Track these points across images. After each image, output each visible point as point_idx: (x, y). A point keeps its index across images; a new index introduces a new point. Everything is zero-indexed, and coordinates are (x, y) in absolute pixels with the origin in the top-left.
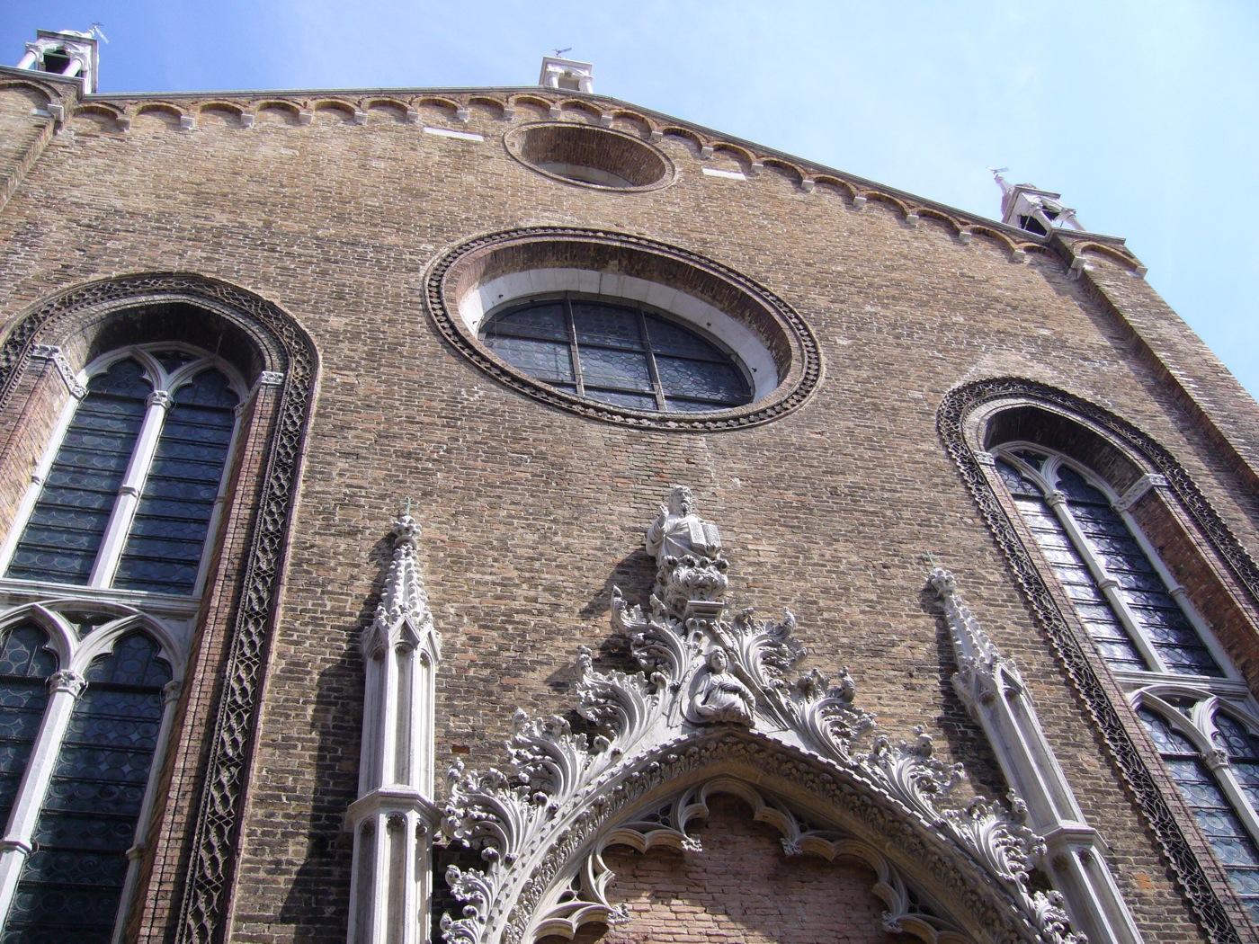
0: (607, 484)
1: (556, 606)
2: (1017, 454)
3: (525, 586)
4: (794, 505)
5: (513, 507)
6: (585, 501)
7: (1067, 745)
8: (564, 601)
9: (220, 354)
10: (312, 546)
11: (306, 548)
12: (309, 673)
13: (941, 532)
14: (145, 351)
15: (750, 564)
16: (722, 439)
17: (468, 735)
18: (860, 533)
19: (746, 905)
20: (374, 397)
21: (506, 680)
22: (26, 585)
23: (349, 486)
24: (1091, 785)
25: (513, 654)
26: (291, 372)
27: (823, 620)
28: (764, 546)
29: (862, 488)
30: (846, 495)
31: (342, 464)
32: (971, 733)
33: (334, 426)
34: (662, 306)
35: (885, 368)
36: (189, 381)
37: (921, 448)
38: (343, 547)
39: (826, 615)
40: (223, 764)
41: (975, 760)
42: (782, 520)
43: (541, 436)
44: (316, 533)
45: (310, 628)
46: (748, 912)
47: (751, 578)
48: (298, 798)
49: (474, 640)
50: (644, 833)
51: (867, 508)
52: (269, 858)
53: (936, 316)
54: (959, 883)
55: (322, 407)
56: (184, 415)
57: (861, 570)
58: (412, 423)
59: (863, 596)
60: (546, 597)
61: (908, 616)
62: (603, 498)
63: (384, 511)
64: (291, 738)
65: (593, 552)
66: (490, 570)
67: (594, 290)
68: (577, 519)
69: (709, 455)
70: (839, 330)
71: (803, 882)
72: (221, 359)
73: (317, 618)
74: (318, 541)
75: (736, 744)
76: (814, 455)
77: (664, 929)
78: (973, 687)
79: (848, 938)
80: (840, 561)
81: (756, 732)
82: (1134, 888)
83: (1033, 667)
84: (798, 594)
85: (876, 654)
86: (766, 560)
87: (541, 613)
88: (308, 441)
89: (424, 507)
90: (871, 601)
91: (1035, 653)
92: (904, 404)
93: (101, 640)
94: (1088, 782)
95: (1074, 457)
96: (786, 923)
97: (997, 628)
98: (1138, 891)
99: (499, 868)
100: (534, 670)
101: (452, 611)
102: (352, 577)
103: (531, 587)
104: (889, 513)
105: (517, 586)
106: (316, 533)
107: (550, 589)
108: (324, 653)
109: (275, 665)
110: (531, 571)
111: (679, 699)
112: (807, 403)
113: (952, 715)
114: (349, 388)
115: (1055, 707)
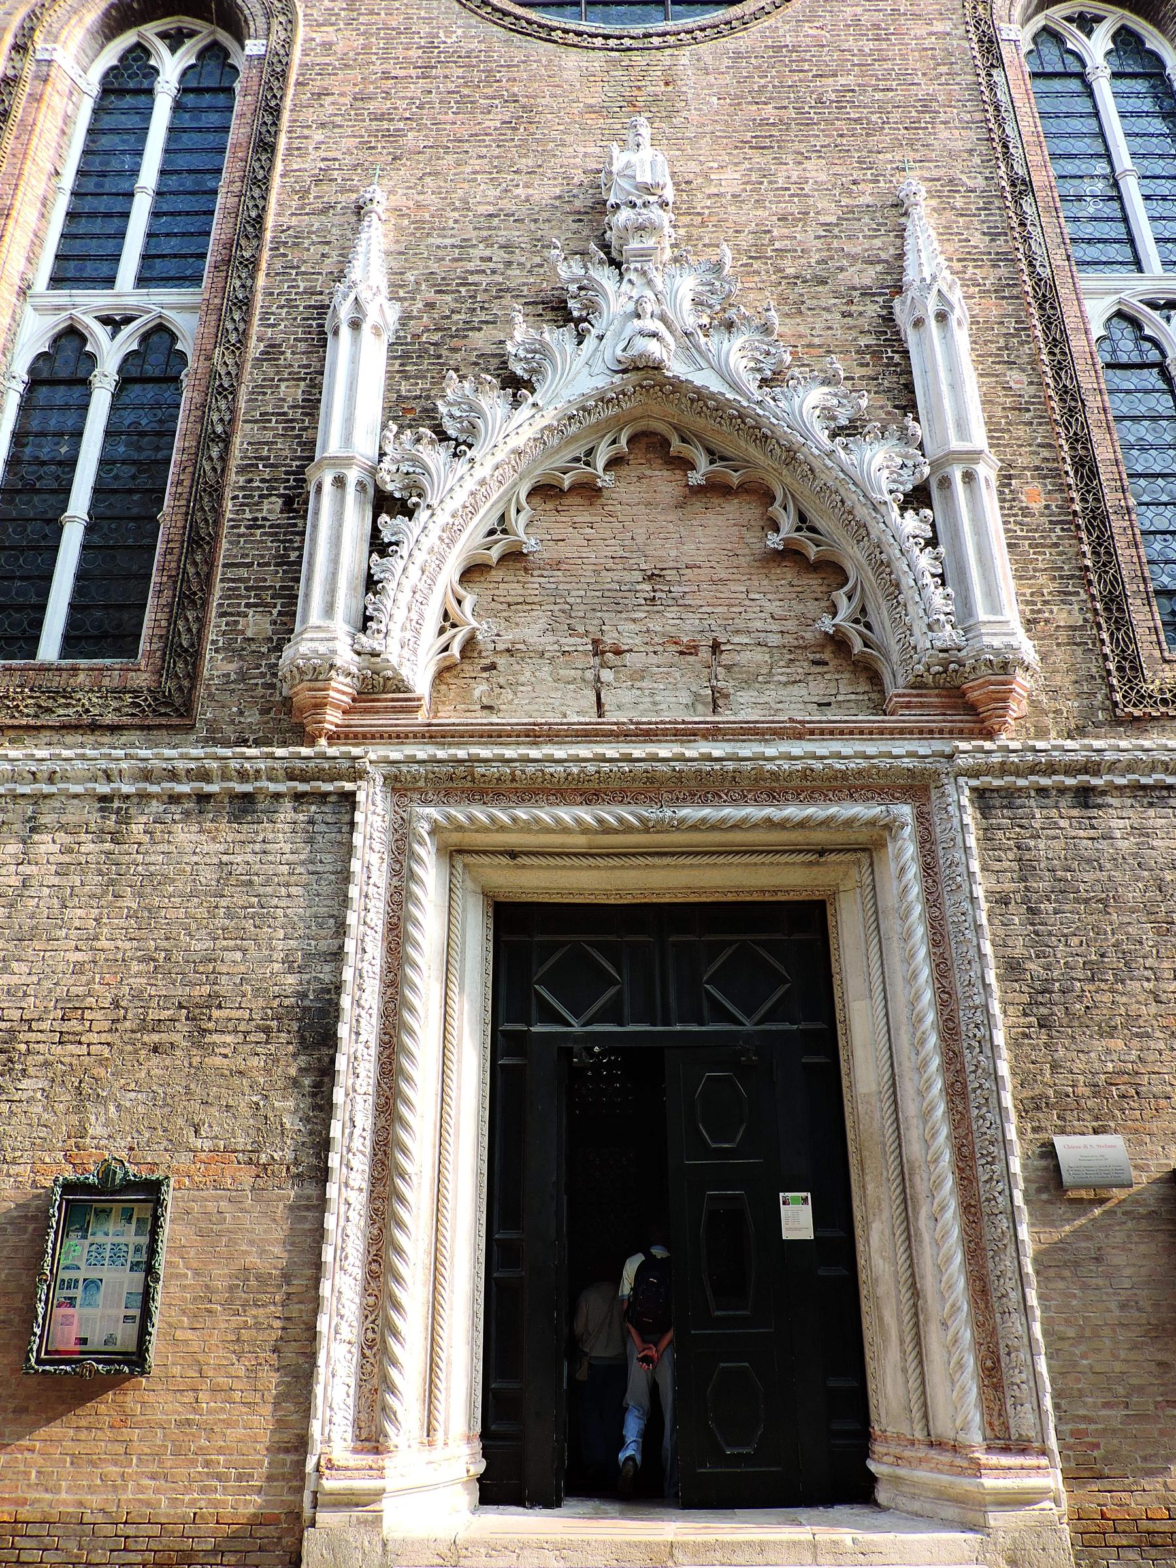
1: (509, 264)
2: (1069, 19)
3: (481, 246)
4: (771, 121)
5: (479, 161)
7: (999, 363)
8: (518, 257)
9: (218, 25)
10: (289, 228)
11: (283, 231)
12: (283, 353)
14: (149, 31)
15: (709, 196)
17: (416, 397)
20: (351, 54)
21: (455, 342)
22: (62, 296)
23: (323, 160)
25: (463, 316)
26: (273, 37)
27: (773, 250)
29: (853, 91)
31: (318, 136)
33: (313, 94)
36: (193, 61)
37: (934, 29)
38: (316, 225)
39: (777, 245)
40: (213, 440)
41: (895, 386)
43: (516, 75)
44: (293, 214)
45: (285, 310)
47: (707, 211)
48: (272, 465)
49: (430, 306)
50: (564, 473)
51: (852, 116)
52: (248, 516)
54: (839, 504)
55: (303, 75)
56: (190, 99)
57: (827, 189)
58: (387, 78)
60: (499, 255)
62: (569, 139)
63: (355, 182)
64: (266, 414)
66: (451, 232)
72: (219, 29)
73: (291, 300)
74: (294, 221)
75: (653, 386)
76: (808, 56)
77: (576, 555)
80: (807, 182)
81: (670, 374)
84: (753, 224)
85: (823, 282)
87: (494, 272)
88: (286, 116)
89: (392, 173)
91: (994, 266)
93: (128, 340)
95: (1138, 13)
98: (1024, 505)
99: (422, 515)
100: (480, 329)
101: (412, 279)
102: (323, 255)
103: (487, 246)
104: (874, 118)
105: (474, 246)
106: (293, 214)
107: (507, 247)
108: (296, 333)
109: (255, 348)
110: (489, 228)
111: (601, 347)
113: (885, 340)
114: (327, 46)
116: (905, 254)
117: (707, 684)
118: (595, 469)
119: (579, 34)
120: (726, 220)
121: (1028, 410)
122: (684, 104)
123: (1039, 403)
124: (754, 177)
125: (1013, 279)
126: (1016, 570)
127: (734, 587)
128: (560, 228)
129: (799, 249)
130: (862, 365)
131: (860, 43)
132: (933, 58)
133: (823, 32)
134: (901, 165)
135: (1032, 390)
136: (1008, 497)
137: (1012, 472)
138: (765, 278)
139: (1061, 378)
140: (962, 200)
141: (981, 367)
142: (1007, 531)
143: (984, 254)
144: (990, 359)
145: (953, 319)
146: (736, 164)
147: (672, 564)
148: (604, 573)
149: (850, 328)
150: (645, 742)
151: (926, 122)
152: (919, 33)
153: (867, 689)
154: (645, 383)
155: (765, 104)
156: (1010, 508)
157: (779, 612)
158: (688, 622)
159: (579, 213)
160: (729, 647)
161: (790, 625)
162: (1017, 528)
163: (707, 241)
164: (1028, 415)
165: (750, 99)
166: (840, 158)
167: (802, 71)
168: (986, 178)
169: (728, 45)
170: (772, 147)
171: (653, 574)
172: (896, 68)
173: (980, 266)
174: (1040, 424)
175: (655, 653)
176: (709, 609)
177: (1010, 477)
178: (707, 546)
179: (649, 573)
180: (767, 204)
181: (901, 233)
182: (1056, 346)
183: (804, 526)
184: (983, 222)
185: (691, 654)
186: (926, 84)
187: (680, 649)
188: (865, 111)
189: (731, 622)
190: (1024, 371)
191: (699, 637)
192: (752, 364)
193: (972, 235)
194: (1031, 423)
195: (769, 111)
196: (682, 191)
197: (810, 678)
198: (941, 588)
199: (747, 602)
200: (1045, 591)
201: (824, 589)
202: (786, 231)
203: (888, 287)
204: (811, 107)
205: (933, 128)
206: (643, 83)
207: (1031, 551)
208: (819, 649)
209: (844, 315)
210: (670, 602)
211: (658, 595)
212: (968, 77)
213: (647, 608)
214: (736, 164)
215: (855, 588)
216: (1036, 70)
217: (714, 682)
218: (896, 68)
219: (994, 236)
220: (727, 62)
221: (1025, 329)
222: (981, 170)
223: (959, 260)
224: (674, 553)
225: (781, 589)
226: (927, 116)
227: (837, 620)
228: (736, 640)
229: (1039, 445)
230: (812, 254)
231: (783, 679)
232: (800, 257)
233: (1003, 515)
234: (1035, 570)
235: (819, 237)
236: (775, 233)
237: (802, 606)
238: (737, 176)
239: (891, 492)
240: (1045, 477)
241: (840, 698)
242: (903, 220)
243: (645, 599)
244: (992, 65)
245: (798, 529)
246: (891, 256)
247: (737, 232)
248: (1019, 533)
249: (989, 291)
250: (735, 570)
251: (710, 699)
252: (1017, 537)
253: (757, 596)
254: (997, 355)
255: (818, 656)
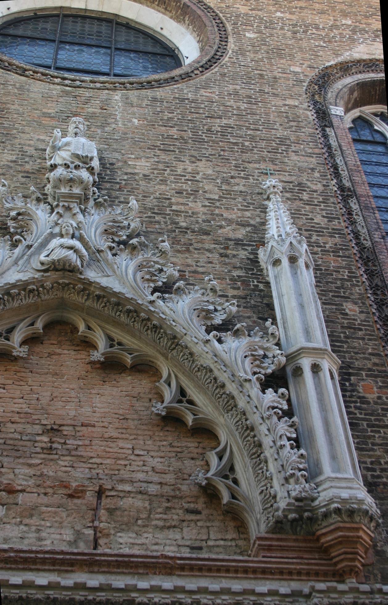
0: (35, 121)
2: (376, 115)
6: (15, 131)
7: (337, 297)
13: (285, 157)
16: (133, 95)
18: (220, 156)
19: (54, 395)
24: (347, 323)
27: (171, 210)
28: (142, 162)
29: (232, 128)
30: (217, 132)
32: (261, 286)
34: (130, 17)
35: (279, 52)
37: (287, 103)
39: (174, 208)
41: (259, 304)
42: (162, 146)
46: (55, 399)
47: (124, 182)
51: (231, 140)
53: (330, 20)
59: (207, 196)
61: (238, 210)
62: (27, 129)
65: (9, 164)
67: (83, 7)
68: (3, 142)
69: (120, 104)
70: (251, 28)
71: (104, 382)
76: (203, 106)
78: (268, 253)
79: (127, 419)
82: (359, 392)
83: (327, 246)
84: (157, 194)
85: (207, 233)
86: (140, 171)
90: (213, 200)
91: (331, 237)
92: (285, 75)
94: (346, 321)
96: (82, 407)
97: (307, 219)
104: (247, 144)
112: (208, 74)
113: (252, 274)
115: (336, 271)
116: (266, 221)
117: (91, 524)
118: (13, 343)
119: (43, 74)
120: (138, 189)
121: (361, 330)
122: (113, 120)
123: (369, 326)
124: (161, 166)
125: (345, 246)
126: (358, 443)
127: (121, 444)
128: (12, 180)
129: (190, 212)
130: (234, 288)
131: (238, 104)
132: (287, 117)
133: (213, 95)
134: (265, 171)
135: (363, 316)
136: (349, 388)
137: (351, 371)
138: (163, 226)
139: (383, 310)
140: (308, 196)
141: (324, 298)
142: (348, 413)
143: (324, 228)
144: (331, 294)
145: (301, 262)
146: (148, 158)
147: (69, 422)
148: (9, 425)
149: (226, 264)
150: (24, 569)
151: (282, 150)
152: (277, 104)
153: (234, 536)
154: (61, 281)
155: (171, 127)
156: (351, 396)
157: (159, 467)
158: (79, 470)
159: (28, 172)
160: (113, 493)
161: (169, 478)
162: (356, 411)
163: (122, 200)
164: (360, 333)
165: (161, 123)
166: (222, 162)
167: (197, 113)
168: (324, 186)
169: (148, 94)
170: (175, 151)
171: (52, 429)
172: (262, 119)
173: (322, 236)
174: (370, 340)
175: (45, 494)
176: (98, 461)
177: (350, 374)
178: (102, 410)
179: (49, 427)
180: (168, 182)
181: (264, 210)
182: (378, 290)
183: (184, 399)
184: (322, 210)
185: (79, 498)
186: (282, 130)
187: (70, 492)
188: (241, 139)
189: (117, 472)
190: (356, 303)
191: (86, 483)
192: (148, 277)
193: (315, 216)
194: (363, 339)
195: (174, 132)
196: (107, 168)
197: (185, 524)
198: (296, 450)
199: (132, 457)
200: (382, 461)
201: (200, 450)
202: (181, 200)
203: (255, 241)
204: (203, 133)
205: (287, 154)
206: (86, 106)
207: (369, 430)
208: (193, 500)
209: (221, 255)
210: (64, 452)
211: (55, 445)
212: (310, 130)
213: (43, 456)
214: (148, 158)
215: (225, 449)
216: (355, 138)
217: (96, 523)
218: (262, 119)
219: (331, 219)
220: (146, 102)
221: (355, 277)
222: (320, 180)
223: (306, 230)
224: (72, 413)
225: (163, 449)
226: (283, 147)
227: (209, 475)
228: (120, 487)
229: (370, 354)
230: (199, 216)
231: (161, 523)
232: (190, 216)
233: (345, 402)
234: (373, 444)
235: (205, 206)
236: (173, 200)
237: (180, 463)
238: (147, 164)
239: (255, 373)
240: (376, 376)
241: (211, 543)
242: (266, 202)
243: (42, 448)
244: (325, 126)
245: (180, 401)
246: (257, 223)
247: (145, 196)
248: (358, 415)
249: (328, 251)
250: (124, 431)
251: (92, 538)
252: (358, 419)
253: (142, 453)
254: (335, 292)
255: (192, 505)
